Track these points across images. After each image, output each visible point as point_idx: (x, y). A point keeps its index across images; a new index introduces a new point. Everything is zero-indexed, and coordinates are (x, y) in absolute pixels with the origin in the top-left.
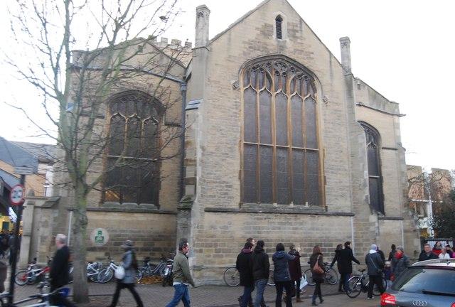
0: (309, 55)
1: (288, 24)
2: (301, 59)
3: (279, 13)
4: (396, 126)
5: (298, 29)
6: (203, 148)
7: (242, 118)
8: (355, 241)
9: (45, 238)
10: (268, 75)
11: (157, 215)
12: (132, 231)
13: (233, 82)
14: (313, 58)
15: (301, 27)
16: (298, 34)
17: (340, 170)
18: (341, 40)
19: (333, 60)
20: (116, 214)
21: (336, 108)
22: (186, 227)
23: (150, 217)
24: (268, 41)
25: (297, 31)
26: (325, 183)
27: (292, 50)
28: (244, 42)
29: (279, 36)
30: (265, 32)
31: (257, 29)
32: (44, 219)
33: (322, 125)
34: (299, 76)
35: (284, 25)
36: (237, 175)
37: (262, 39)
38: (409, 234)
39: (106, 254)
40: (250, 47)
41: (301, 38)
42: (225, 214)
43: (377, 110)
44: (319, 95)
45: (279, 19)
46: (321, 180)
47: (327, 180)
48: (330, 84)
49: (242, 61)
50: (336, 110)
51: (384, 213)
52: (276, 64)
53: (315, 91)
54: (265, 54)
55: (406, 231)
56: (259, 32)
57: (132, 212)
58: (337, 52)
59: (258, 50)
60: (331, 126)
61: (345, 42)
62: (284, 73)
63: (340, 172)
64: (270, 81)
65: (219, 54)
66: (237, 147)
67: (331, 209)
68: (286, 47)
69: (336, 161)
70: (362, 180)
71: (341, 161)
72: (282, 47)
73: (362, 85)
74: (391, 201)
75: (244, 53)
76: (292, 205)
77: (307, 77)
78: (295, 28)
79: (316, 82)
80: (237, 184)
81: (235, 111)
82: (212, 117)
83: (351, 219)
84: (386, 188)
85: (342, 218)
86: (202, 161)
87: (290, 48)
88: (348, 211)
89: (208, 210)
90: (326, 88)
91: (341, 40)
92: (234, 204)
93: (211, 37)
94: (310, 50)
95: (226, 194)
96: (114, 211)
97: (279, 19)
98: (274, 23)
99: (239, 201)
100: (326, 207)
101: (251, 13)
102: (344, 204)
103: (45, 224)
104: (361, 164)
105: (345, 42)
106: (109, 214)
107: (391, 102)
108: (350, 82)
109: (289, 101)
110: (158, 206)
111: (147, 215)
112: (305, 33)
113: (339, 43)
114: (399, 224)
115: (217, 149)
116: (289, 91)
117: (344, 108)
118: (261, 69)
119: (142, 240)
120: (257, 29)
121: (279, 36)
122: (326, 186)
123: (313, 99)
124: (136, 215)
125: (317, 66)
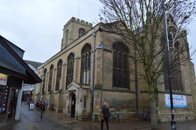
9: (98, 102)
11: (129, 93)
12: (122, 100)
20: (117, 92)
23: (125, 94)
39: (115, 109)
46: (183, 82)
57: (122, 91)
67: (186, 94)
76: (176, 91)
83: (191, 97)
96: (117, 91)
106: (115, 92)
110: (130, 89)
111: (127, 93)
119: (126, 103)
124: (123, 93)
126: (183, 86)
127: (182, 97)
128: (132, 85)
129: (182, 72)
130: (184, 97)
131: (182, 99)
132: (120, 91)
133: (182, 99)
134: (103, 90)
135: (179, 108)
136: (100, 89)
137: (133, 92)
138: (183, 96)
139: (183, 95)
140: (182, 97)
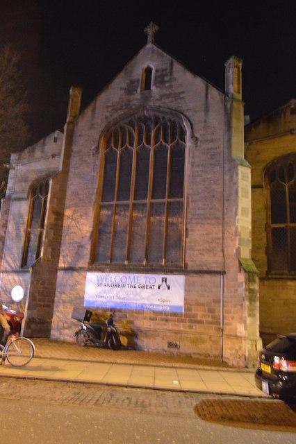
13: (93, 147)
14: (183, 98)
16: (166, 78)
17: (209, 218)
24: (132, 97)
25: (167, 75)
26: (187, 236)
27: (157, 97)
28: (107, 107)
31: (121, 89)
40: (112, 110)
47: (190, 233)
49: (103, 126)
50: (211, 149)
59: (120, 109)
63: (209, 221)
68: (151, 97)
69: (204, 209)
71: (211, 209)
75: (106, 118)
78: (164, 72)
85: (207, 277)
94: (180, 90)
102: (211, 261)
120: (121, 89)
122: (188, 240)
127: (165, 280)
130: (177, 281)
139: (172, 272)
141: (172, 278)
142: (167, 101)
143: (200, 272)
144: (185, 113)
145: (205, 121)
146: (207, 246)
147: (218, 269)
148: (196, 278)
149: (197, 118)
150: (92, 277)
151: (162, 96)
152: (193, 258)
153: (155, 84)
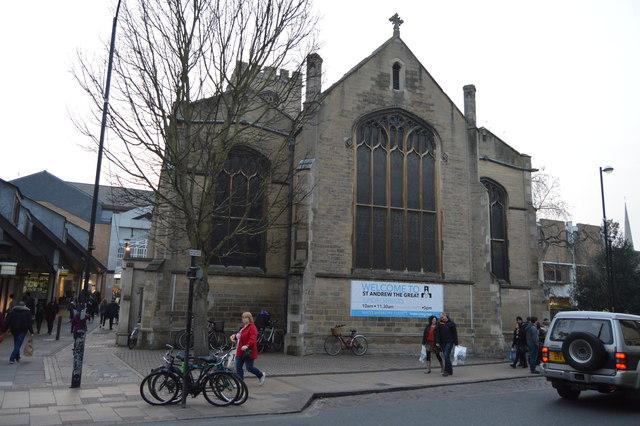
0: (428, 107)
1: (407, 72)
2: (419, 112)
3: (397, 60)
4: (527, 183)
5: (417, 77)
6: (314, 211)
7: (355, 178)
8: (474, 311)
9: (150, 302)
10: (383, 131)
12: (237, 296)
15: (420, 76)
16: (416, 83)
18: (465, 88)
19: (455, 112)
20: (220, 278)
21: (457, 165)
22: (298, 293)
23: (257, 281)
25: (416, 80)
26: (443, 249)
27: (410, 102)
28: (358, 95)
29: (396, 86)
30: (381, 82)
31: (372, 79)
32: (148, 283)
33: (440, 185)
34: (417, 131)
35: (402, 73)
36: (349, 239)
37: (378, 91)
38: (538, 306)
41: (421, 88)
42: (336, 280)
43: (506, 166)
44: (438, 151)
45: (396, 67)
48: (451, 141)
49: (355, 117)
51: (508, 281)
52: (392, 118)
53: (434, 146)
54: (380, 107)
55: (534, 302)
56: (374, 83)
57: (238, 275)
58: (460, 102)
60: (450, 186)
61: (470, 91)
62: (400, 128)
64: (386, 138)
65: (331, 110)
66: (349, 210)
70: (483, 246)
72: (399, 98)
73: (487, 135)
74: (517, 268)
75: (358, 107)
76: (406, 272)
77: (426, 133)
79: (436, 137)
80: (349, 249)
81: (347, 170)
82: (324, 177)
84: (512, 253)
86: (313, 224)
87: (407, 99)
88: (466, 278)
89: (319, 276)
90: (447, 144)
91: (465, 88)
92: (346, 269)
93: (324, 88)
94: (431, 101)
95: (337, 259)
97: (396, 67)
98: (390, 72)
99: (350, 267)
100: (443, 274)
101: (366, 61)
102: (464, 272)
103: (150, 288)
104: (483, 228)
105: (470, 91)
107: (523, 156)
108: (478, 136)
109: (405, 159)
110: (265, 270)
112: (426, 82)
113: (463, 92)
114: (527, 295)
115: (329, 211)
116: (405, 147)
117: (465, 166)
118: (376, 124)
120: (372, 79)
121: (396, 86)
123: (431, 157)
124: (242, 279)
125: (438, 119)
126: (438, 258)
127: (426, 288)
128: (274, 262)
129: (439, 214)
130: (437, 289)
131: (426, 296)
132: (229, 275)
133: (426, 296)
134: (174, 273)
135: (406, 319)
136: (155, 271)
137: (275, 277)
138: (431, 286)
139: (433, 282)
140: (426, 288)
141: (432, 287)
142: (419, 109)
143: (455, 283)
144: (435, 127)
145: (453, 141)
146: (459, 258)
147: (467, 280)
148: (452, 288)
149: (446, 134)
150: (357, 286)
151: (414, 102)
152: (451, 269)
153: (389, 76)
